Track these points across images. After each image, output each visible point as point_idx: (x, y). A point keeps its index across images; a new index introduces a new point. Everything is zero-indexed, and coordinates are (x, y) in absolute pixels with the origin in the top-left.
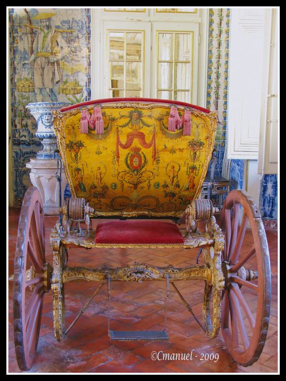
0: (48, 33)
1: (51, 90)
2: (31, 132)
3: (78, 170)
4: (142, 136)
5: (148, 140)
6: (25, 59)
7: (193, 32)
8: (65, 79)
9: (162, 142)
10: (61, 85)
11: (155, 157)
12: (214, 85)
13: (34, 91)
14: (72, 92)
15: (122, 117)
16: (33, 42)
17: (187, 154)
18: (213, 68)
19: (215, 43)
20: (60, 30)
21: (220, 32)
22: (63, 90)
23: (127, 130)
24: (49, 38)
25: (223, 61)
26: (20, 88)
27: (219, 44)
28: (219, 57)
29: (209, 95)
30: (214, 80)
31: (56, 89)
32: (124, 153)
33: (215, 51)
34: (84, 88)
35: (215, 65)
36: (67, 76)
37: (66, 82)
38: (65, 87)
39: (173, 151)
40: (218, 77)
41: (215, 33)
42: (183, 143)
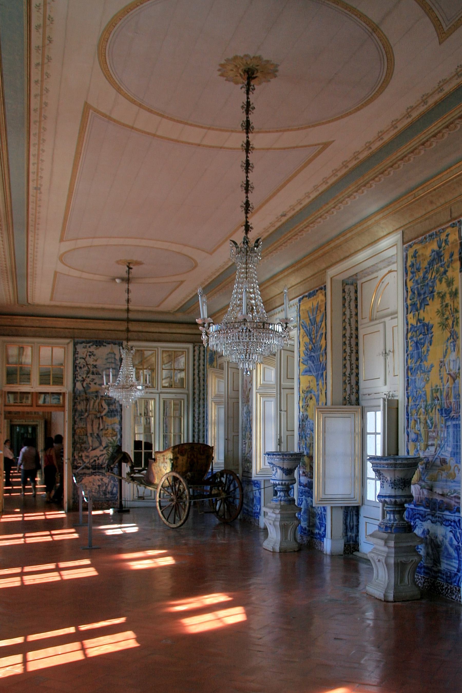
1: (98, 435)
6: (82, 415)
7: (183, 399)
8: (106, 428)
10: (104, 432)
12: (196, 430)
13: (86, 435)
14: (111, 435)
20: (104, 398)
21: (200, 399)
22: (105, 434)
24: (97, 404)
25: (201, 416)
26: (78, 433)
27: (199, 406)
28: (199, 413)
31: (101, 433)
34: (118, 433)
35: (197, 418)
36: (108, 425)
37: (107, 429)
38: (106, 432)
40: (199, 426)
41: (197, 399)
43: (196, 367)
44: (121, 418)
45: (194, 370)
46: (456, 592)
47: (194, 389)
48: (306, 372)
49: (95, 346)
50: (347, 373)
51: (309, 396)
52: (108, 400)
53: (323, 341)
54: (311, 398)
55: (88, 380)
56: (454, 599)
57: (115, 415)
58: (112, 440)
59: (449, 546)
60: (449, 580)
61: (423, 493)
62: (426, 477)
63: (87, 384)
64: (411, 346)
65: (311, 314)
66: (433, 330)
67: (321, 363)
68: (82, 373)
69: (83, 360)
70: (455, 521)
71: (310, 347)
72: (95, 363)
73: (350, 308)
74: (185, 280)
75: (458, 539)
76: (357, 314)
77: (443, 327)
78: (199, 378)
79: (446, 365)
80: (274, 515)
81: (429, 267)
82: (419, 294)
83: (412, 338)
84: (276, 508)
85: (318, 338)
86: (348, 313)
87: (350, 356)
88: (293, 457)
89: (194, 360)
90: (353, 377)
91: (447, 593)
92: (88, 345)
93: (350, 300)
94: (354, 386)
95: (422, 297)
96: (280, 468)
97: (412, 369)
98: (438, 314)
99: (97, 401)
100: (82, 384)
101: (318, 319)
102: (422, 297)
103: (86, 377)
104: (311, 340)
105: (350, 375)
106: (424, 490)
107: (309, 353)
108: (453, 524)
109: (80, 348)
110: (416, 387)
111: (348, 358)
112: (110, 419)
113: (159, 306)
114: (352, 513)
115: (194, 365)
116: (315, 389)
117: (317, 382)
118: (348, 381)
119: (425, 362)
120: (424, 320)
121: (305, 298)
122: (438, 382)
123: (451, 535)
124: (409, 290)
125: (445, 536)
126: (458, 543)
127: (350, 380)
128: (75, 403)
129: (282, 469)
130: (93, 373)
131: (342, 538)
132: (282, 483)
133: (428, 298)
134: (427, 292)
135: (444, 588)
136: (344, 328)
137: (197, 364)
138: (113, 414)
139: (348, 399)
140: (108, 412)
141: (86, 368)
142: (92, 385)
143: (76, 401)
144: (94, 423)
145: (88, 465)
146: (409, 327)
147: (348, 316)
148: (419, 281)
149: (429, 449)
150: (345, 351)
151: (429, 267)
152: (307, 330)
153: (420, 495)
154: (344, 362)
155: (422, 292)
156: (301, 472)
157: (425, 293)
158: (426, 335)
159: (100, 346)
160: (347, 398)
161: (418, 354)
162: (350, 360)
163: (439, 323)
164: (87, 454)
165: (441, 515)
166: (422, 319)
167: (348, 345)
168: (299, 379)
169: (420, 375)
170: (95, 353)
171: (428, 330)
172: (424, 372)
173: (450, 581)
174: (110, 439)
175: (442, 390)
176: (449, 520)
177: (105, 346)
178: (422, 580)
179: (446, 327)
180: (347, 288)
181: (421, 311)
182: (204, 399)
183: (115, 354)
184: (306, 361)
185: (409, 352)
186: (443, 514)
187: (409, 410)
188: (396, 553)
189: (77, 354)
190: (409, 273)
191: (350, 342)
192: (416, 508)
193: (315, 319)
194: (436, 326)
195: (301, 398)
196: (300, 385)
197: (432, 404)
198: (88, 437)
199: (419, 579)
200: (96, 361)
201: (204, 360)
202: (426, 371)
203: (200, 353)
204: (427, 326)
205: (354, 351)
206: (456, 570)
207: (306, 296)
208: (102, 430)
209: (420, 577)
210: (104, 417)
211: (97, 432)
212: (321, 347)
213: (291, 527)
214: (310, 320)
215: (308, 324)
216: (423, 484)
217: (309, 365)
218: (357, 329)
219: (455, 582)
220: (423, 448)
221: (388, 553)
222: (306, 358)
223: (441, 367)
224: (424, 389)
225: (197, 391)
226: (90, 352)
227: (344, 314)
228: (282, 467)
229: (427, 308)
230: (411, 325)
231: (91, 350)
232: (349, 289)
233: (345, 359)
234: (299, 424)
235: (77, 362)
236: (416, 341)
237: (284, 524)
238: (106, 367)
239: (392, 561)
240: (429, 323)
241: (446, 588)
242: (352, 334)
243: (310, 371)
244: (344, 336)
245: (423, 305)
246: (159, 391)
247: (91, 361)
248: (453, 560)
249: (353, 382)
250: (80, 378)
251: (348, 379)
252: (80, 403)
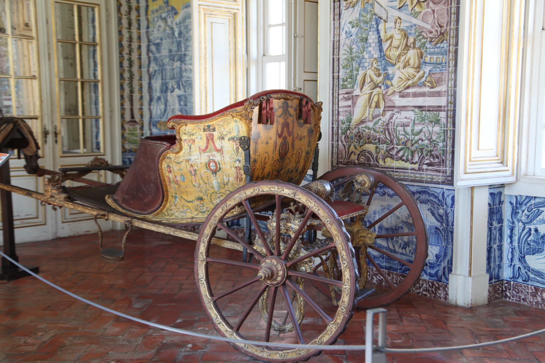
12: (126, 75)
19: (125, 22)
27: (130, 24)
28: (130, 39)
30: (127, 69)
33: (125, 32)
35: (126, 50)
40: (131, 65)
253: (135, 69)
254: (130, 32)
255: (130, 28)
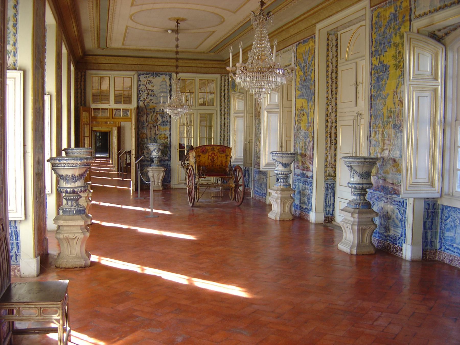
0: (154, 114)
1: (154, 138)
2: (145, 156)
3: (199, 162)
4: (214, 154)
5: (216, 154)
8: (160, 133)
9: (219, 155)
10: (159, 136)
11: (217, 159)
12: (222, 135)
13: (147, 138)
14: (163, 139)
15: (210, 149)
16: (147, 118)
17: (225, 158)
18: (222, 128)
20: (159, 113)
21: (225, 113)
23: (211, 152)
25: (226, 125)
27: (225, 119)
28: (225, 123)
29: (220, 140)
31: (156, 137)
32: (210, 158)
33: (223, 122)
34: (168, 137)
35: (223, 127)
36: (161, 132)
38: (160, 136)
39: (221, 157)
40: (224, 132)
41: (223, 114)
42: (224, 155)
43: (222, 91)
44: (171, 127)
45: (221, 93)
46: (399, 250)
47: (221, 106)
48: (300, 96)
49: (152, 77)
50: (329, 98)
51: (302, 113)
52: (161, 114)
53: (313, 75)
54: (304, 115)
55: (148, 100)
56: (398, 255)
57: (166, 125)
58: (164, 142)
59: (396, 219)
60: (395, 242)
61: (379, 182)
62: (382, 171)
63: (147, 103)
64: (374, 80)
65: (304, 56)
66: (390, 69)
67: (311, 90)
68: (144, 95)
69: (144, 86)
70: (400, 202)
71: (303, 78)
72: (152, 88)
73: (332, 51)
74: (216, 31)
75: (402, 214)
76: (337, 56)
77: (396, 67)
78: (225, 99)
79: (398, 94)
80: (276, 195)
81: (388, 24)
82: (381, 44)
83: (375, 74)
84: (278, 190)
85: (309, 73)
86: (330, 55)
87: (332, 86)
88: (289, 155)
89: (221, 86)
90: (333, 100)
91: (393, 250)
92: (148, 76)
93: (333, 46)
94: (334, 107)
95: (383, 46)
96: (280, 163)
97: (374, 96)
98: (393, 58)
99: (154, 115)
100: (144, 103)
101: (310, 59)
102: (383, 46)
103: (146, 98)
104: (304, 73)
105: (331, 98)
106: (380, 180)
107: (302, 83)
108: (399, 204)
109: (142, 77)
110: (376, 109)
111: (330, 87)
112: (163, 127)
113: (197, 48)
114: (330, 195)
115: (221, 90)
116: (306, 108)
117: (308, 103)
118: (330, 103)
119: (383, 92)
120: (383, 62)
121: (300, 44)
122: (392, 106)
123: (398, 211)
124: (374, 40)
125: (393, 212)
126: (402, 217)
127: (331, 102)
128: (139, 116)
129: (282, 164)
130: (151, 96)
131: (323, 212)
132: (281, 173)
133: (387, 47)
134: (386, 42)
135: (391, 247)
136: (328, 66)
137: (223, 89)
138: (165, 124)
139: (329, 116)
140: (162, 122)
141: (146, 92)
142: (151, 104)
143: (140, 114)
144: (152, 130)
145: (148, 159)
146: (373, 67)
147: (331, 57)
148: (381, 35)
149: (384, 152)
150: (328, 82)
151: (388, 24)
152: (302, 66)
153: (377, 183)
154: (327, 90)
155: (383, 42)
156: (295, 166)
157: (384, 43)
158: (384, 72)
159: (156, 76)
160: (328, 114)
161: (379, 85)
162: (332, 88)
163: (394, 65)
164: (147, 151)
165: (391, 198)
166: (382, 61)
167: (330, 78)
168: (295, 101)
169: (380, 100)
170: (152, 81)
171: (386, 69)
172: (382, 98)
173: (395, 243)
174: (163, 141)
175: (395, 111)
176: (396, 201)
177: (160, 76)
178: (376, 241)
179: (398, 67)
180: (330, 37)
181: (382, 56)
182: (228, 114)
183: (166, 82)
184: (301, 88)
185: (372, 84)
186: (392, 197)
187: (372, 124)
188: (359, 222)
189: (141, 82)
190: (374, 28)
191: (332, 76)
192: (374, 192)
193: (307, 59)
194: (392, 66)
195: (297, 114)
196: (296, 105)
197: (387, 121)
198: (148, 140)
199: (375, 241)
200: (153, 87)
201: (228, 86)
202: (384, 98)
203: (225, 81)
204: (386, 66)
205: (335, 82)
206: (400, 235)
207: (301, 43)
208: (157, 135)
209: (375, 240)
210: (159, 126)
211: (154, 136)
212: (311, 78)
213: (288, 203)
214: (304, 60)
215: (302, 62)
216: (380, 176)
217: (302, 91)
218: (337, 67)
219: (399, 243)
220: (380, 151)
221: (354, 222)
222: (300, 86)
223: (394, 95)
224: (382, 111)
225: (223, 108)
226: (149, 81)
227: (328, 56)
228: (282, 162)
229: (387, 53)
230: (375, 65)
231: (150, 80)
232: (332, 38)
233: (328, 87)
234: (295, 133)
235: (140, 87)
236: (377, 77)
237: (283, 202)
238: (159, 91)
239: (356, 228)
240: (387, 64)
241: (393, 247)
242: (333, 70)
243: (303, 96)
244: (328, 71)
245: (383, 51)
246: (197, 108)
247: (149, 86)
248: (398, 228)
249: (333, 104)
250: (142, 99)
251: (330, 101)
252: (142, 116)
253: (226, 133)
254: (224, 122)
255: (225, 120)
